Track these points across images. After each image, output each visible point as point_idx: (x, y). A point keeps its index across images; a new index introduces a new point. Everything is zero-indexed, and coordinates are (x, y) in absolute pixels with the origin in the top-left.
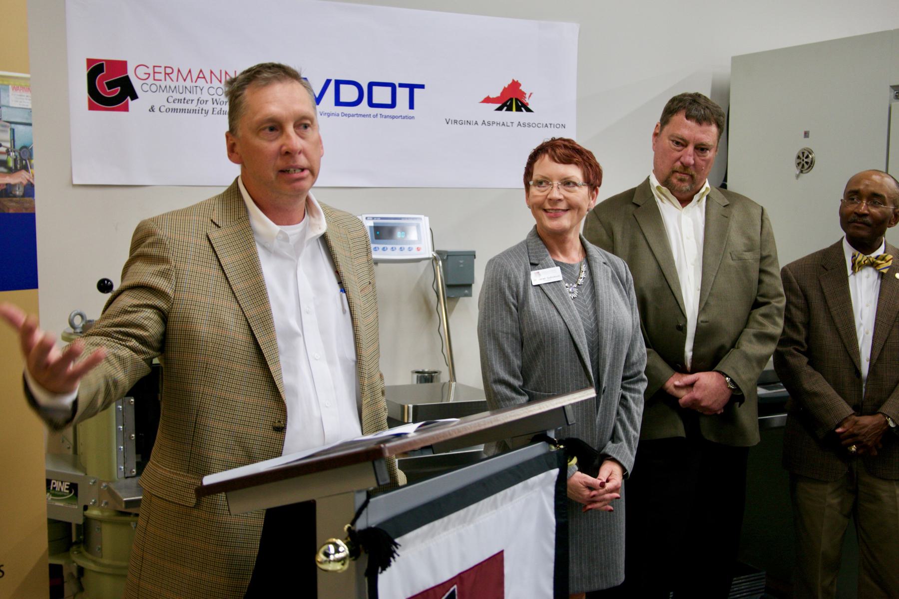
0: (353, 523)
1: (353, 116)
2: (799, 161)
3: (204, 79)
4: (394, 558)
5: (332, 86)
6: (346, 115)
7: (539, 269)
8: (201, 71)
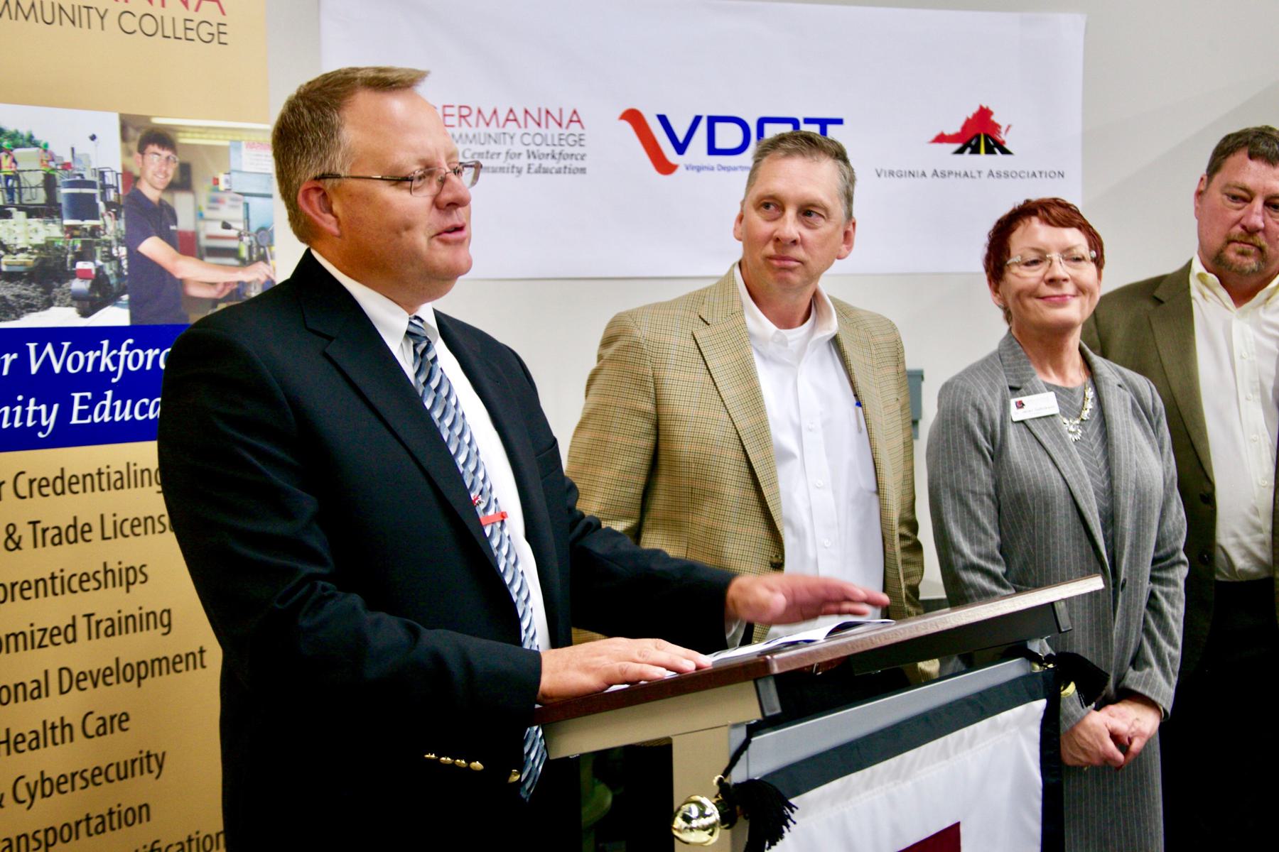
0: (727, 772)
1: (735, 169)
3: (514, 124)
4: (788, 826)
5: (702, 128)
6: (724, 168)
7: (1021, 396)
8: (511, 111)
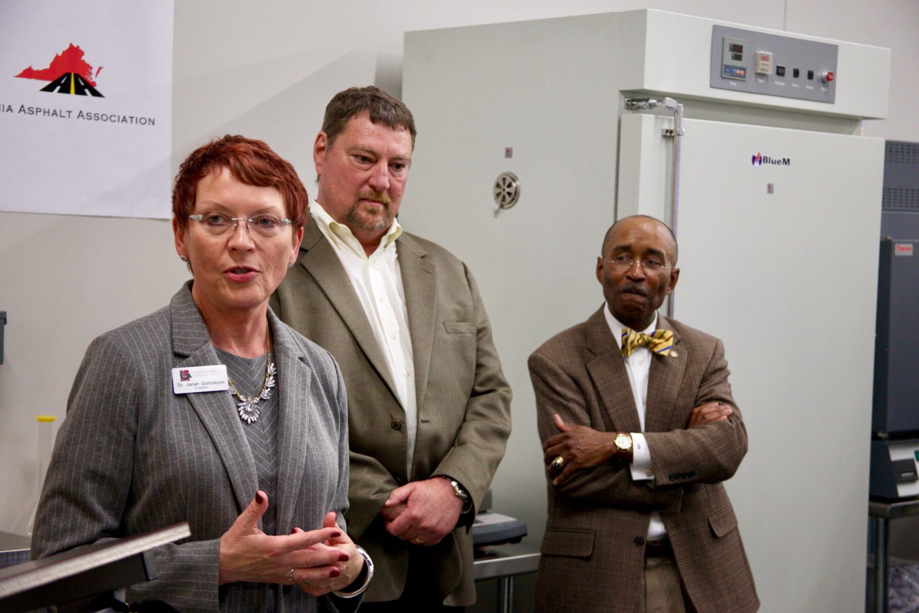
2: (498, 190)
